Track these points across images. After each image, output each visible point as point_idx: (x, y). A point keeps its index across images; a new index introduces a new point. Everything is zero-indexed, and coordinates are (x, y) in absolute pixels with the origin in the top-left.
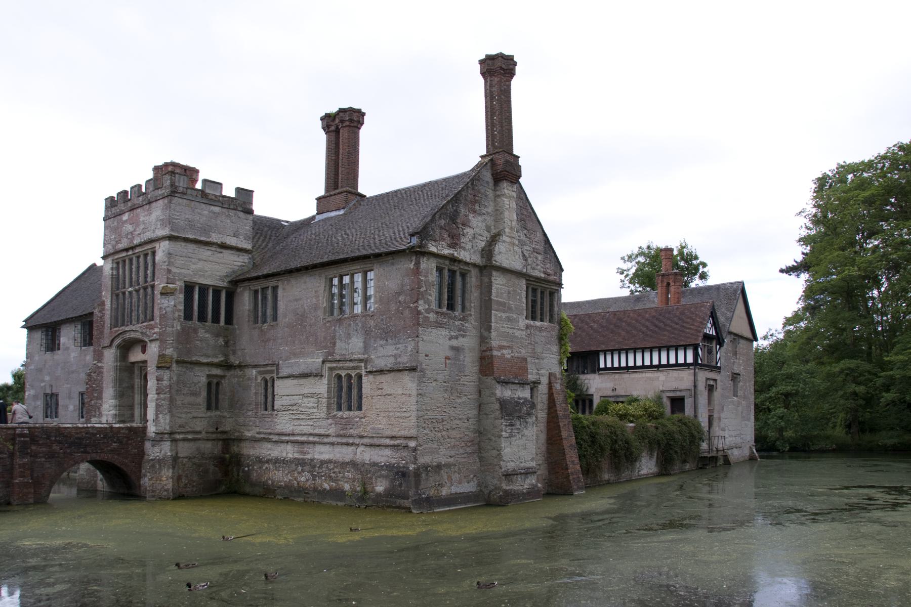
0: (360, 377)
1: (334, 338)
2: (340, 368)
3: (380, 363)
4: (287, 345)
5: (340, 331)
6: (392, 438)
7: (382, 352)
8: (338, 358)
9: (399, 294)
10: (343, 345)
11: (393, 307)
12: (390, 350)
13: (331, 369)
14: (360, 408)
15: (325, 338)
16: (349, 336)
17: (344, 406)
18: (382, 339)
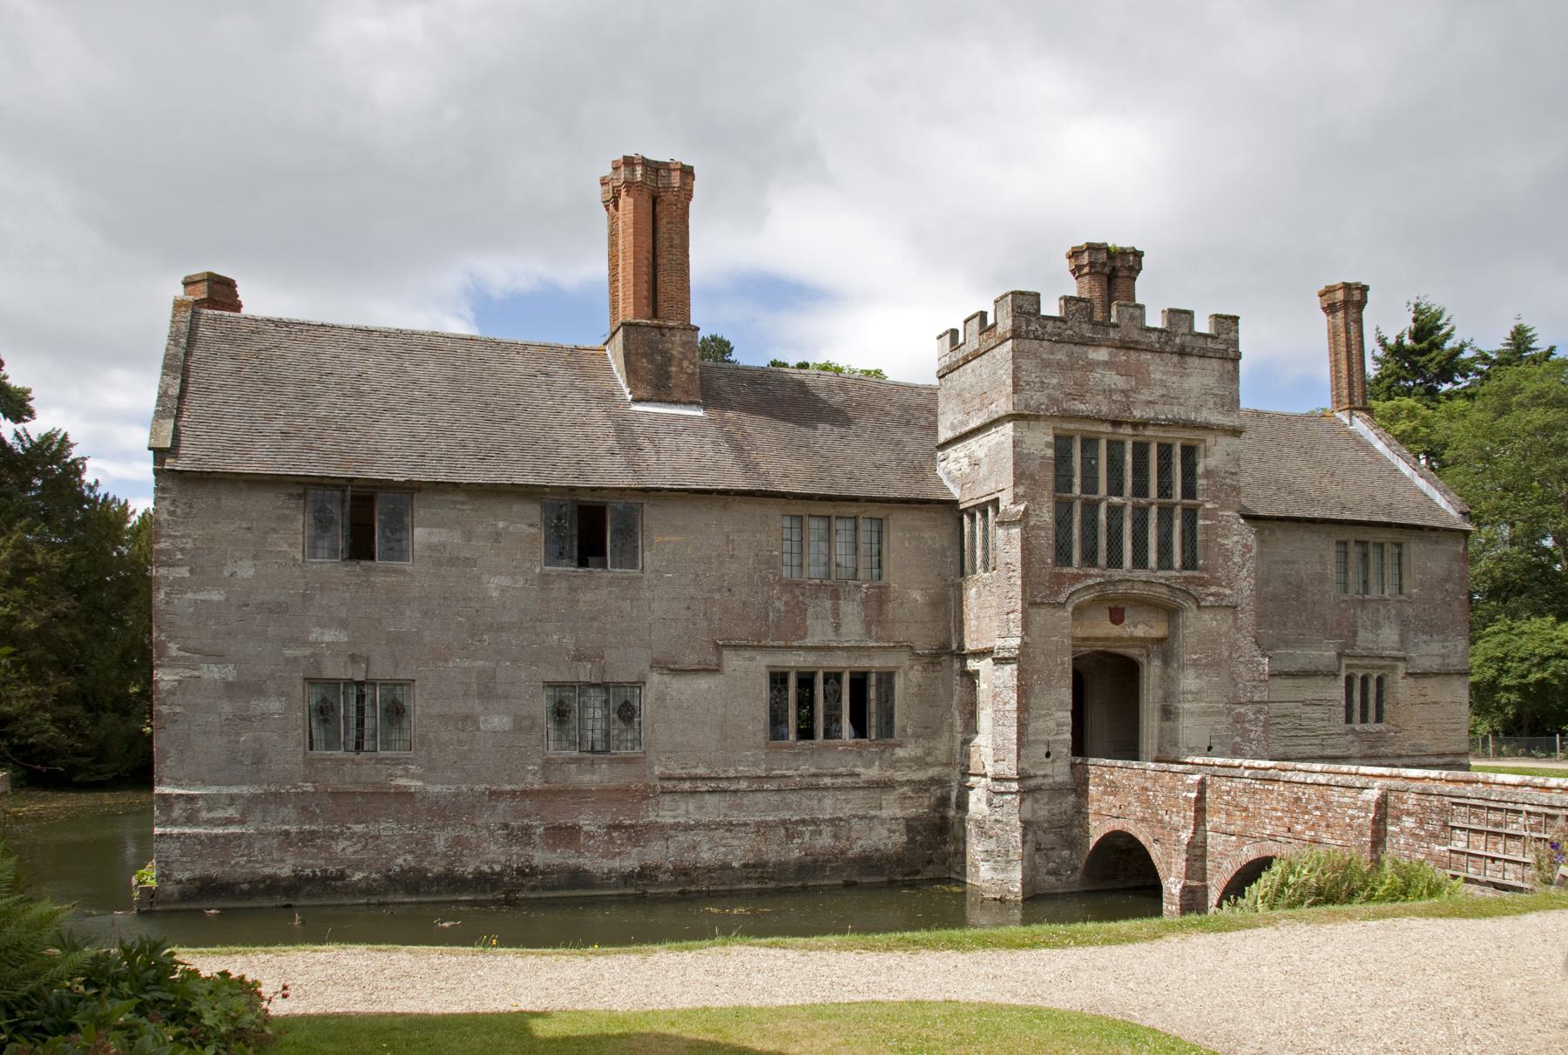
0: (1380, 680)
1: (1354, 624)
2: (1359, 667)
3: (1423, 664)
4: (1271, 627)
5: (1363, 617)
6: (1439, 755)
7: (1424, 649)
8: (1358, 651)
9: (1446, 581)
10: (1370, 636)
11: (1438, 596)
12: (1436, 648)
13: (1348, 666)
14: (1379, 719)
15: (1339, 624)
16: (1377, 625)
17: (1357, 716)
18: (1424, 633)
